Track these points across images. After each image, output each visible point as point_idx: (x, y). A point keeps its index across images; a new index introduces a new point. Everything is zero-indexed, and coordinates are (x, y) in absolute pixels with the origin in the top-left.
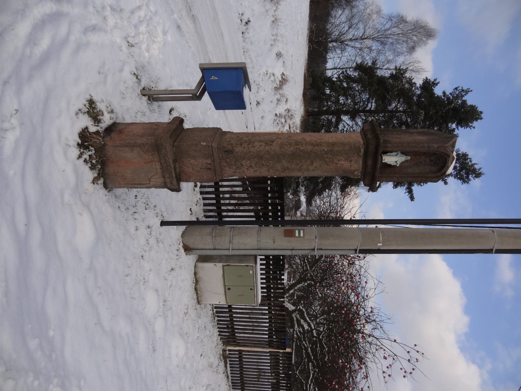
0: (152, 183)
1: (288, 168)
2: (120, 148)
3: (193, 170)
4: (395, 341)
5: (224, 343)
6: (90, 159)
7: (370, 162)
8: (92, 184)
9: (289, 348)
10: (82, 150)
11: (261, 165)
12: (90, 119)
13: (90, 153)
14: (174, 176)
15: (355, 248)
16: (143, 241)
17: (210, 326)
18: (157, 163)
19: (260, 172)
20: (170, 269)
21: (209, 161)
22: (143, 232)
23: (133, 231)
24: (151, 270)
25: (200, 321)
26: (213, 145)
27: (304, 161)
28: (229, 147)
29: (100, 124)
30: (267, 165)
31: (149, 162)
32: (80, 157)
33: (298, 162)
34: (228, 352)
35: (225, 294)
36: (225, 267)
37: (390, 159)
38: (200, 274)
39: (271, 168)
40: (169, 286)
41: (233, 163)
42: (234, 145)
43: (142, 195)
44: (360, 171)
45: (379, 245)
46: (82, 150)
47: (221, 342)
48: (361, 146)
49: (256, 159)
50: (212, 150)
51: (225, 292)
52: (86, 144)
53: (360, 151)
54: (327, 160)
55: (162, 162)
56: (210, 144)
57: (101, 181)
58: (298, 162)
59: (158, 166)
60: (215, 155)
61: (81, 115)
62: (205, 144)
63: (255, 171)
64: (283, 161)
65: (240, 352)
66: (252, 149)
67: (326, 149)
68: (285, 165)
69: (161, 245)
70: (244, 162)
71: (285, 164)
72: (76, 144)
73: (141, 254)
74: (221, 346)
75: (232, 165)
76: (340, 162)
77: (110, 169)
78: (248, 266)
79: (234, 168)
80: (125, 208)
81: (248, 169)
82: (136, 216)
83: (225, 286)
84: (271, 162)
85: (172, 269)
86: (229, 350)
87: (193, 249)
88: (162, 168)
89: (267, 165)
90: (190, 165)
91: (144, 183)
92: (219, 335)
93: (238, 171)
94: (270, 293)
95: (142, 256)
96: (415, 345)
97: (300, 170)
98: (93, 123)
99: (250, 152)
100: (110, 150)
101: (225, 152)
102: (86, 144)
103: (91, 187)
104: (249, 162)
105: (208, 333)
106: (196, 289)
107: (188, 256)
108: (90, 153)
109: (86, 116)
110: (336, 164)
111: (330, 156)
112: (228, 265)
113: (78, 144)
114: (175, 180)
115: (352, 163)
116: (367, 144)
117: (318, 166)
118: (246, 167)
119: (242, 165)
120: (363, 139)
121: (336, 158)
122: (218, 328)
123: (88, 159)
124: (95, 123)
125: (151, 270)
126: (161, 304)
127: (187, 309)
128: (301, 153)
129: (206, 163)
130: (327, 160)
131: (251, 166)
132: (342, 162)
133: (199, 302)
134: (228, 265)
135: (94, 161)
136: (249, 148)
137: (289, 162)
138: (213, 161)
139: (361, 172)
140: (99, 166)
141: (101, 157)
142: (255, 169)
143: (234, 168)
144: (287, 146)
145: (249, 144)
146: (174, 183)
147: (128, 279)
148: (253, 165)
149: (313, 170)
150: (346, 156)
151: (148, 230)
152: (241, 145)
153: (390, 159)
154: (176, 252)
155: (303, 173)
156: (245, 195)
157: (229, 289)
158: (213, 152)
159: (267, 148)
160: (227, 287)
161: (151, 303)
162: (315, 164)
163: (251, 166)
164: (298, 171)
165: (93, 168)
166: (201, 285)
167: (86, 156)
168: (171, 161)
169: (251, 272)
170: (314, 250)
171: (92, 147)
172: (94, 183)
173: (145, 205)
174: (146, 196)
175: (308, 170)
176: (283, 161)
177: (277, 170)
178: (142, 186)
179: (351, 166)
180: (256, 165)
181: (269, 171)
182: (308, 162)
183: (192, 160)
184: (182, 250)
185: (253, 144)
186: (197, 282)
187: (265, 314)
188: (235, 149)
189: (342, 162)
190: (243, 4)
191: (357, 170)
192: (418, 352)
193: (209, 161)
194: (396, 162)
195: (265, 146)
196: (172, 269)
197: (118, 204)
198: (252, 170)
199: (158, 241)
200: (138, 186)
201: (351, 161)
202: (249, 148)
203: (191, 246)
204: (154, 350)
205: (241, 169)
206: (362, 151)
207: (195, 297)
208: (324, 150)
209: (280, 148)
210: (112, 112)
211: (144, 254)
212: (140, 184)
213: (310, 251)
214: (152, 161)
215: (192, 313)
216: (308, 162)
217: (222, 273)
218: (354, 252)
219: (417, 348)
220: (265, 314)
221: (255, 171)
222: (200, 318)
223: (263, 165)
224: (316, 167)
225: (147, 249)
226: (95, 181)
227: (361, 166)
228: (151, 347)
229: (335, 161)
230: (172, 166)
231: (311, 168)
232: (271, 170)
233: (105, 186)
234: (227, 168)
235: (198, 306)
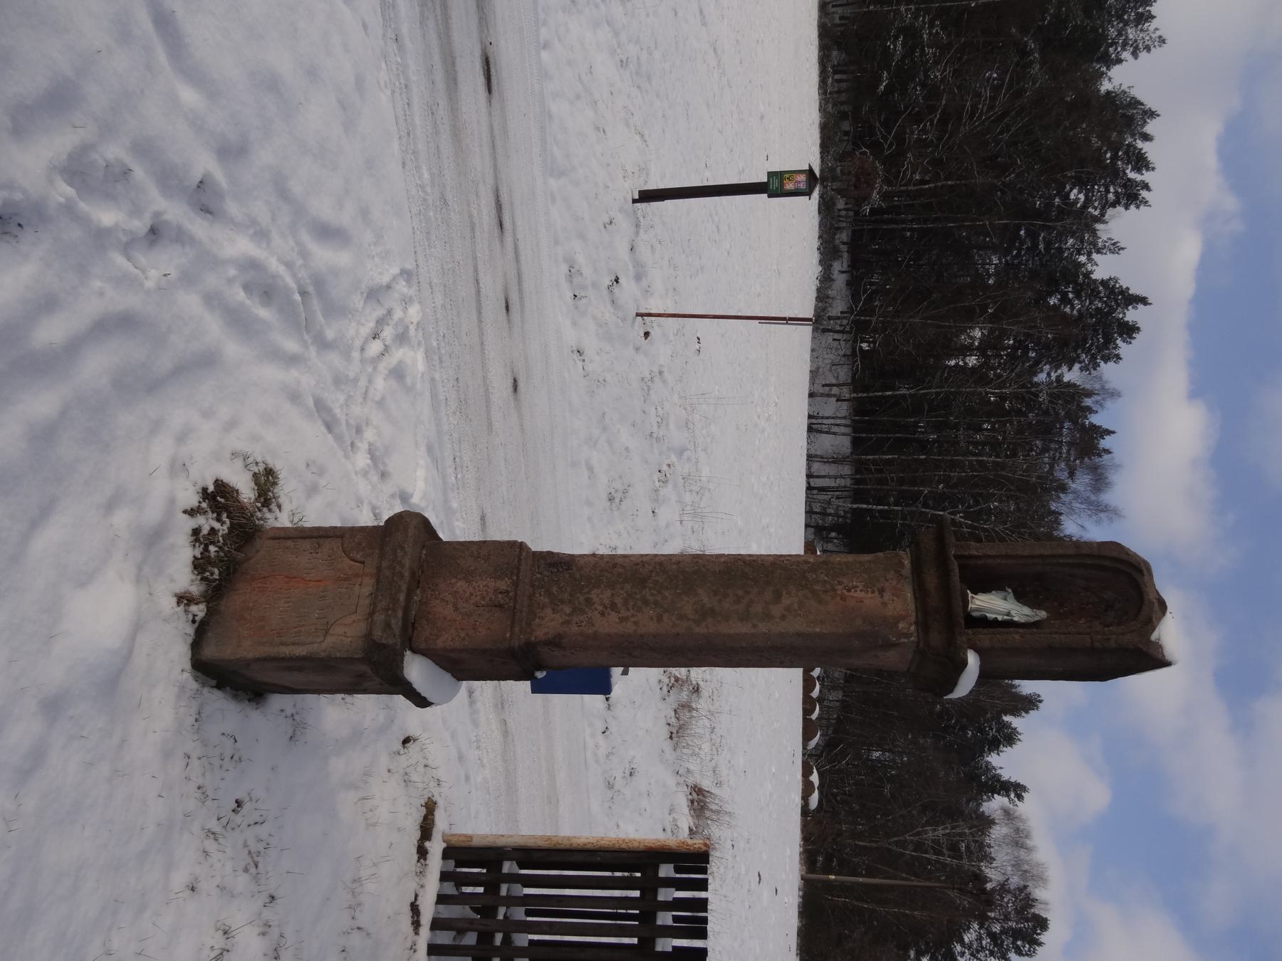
1: (712, 610)
2: (290, 543)
3: (456, 609)
7: (931, 581)
8: (175, 600)
10: (204, 505)
11: (639, 603)
12: (253, 484)
13: (217, 525)
19: (636, 623)
21: (503, 585)
29: (265, 510)
31: (345, 580)
32: (191, 512)
33: (740, 592)
41: (566, 596)
43: (256, 817)
44: (913, 619)
46: (204, 505)
49: (628, 586)
50: (520, 554)
53: (902, 565)
55: (385, 564)
57: (199, 610)
58: (740, 592)
60: (523, 568)
61: (239, 463)
64: (700, 591)
70: (594, 596)
71: (706, 600)
72: (200, 485)
75: (562, 602)
77: (234, 601)
81: (603, 614)
84: (666, 593)
89: (656, 603)
90: (449, 598)
93: (575, 619)
97: (744, 618)
103: (168, 603)
104: (608, 593)
108: (217, 525)
109: (249, 476)
110: (843, 598)
113: (205, 490)
115: (887, 596)
118: (600, 608)
119: (589, 602)
121: (840, 583)
123: (205, 531)
129: (496, 591)
130: (817, 587)
131: (613, 606)
137: (715, 593)
138: (516, 584)
139: (916, 623)
142: (624, 613)
143: (568, 610)
148: (619, 601)
149: (783, 617)
155: (754, 626)
158: (520, 560)
162: (786, 601)
163: (613, 606)
164: (742, 620)
165: (199, 565)
167: (206, 522)
173: (249, 860)
174: (262, 831)
175: (767, 616)
176: (700, 591)
177: (682, 617)
179: (884, 604)
180: (626, 602)
181: (660, 619)
190: (621, 825)
191: (903, 618)
193: (503, 585)
198: (613, 617)
201: (882, 591)
205: (583, 612)
212: (294, 644)
214: (357, 575)
221: (622, 620)
223: (646, 602)
224: (788, 609)
226: (184, 599)
227: (912, 606)
231: (776, 610)
232: (666, 616)
234: (548, 611)
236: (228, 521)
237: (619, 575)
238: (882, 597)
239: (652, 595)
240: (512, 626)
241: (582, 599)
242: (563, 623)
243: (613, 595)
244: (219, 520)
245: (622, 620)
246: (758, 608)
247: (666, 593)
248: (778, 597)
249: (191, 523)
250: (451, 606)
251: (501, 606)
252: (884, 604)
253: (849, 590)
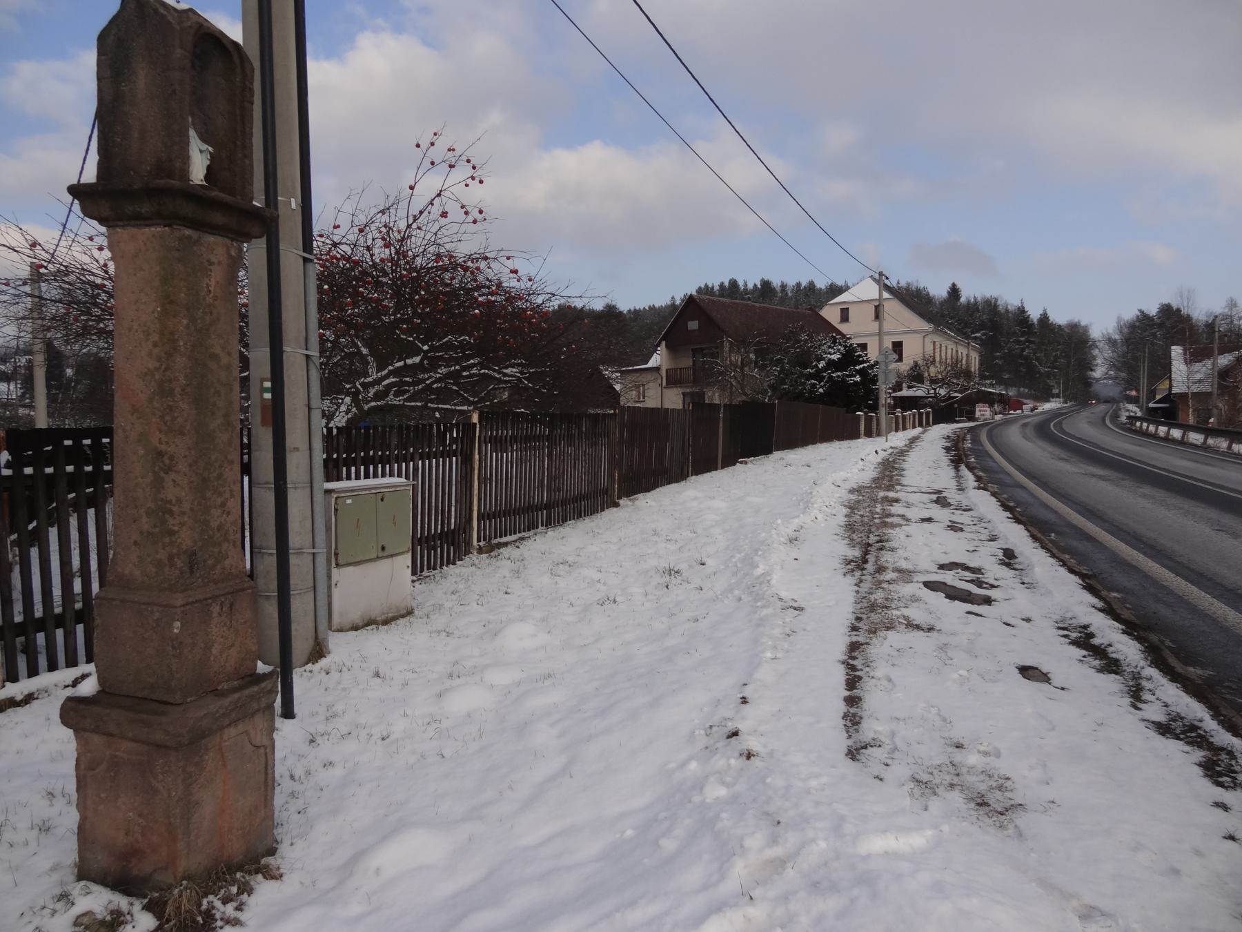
0: (266, 742)
3: (233, 645)
4: (412, 188)
5: (468, 552)
6: (231, 900)
7: (218, 218)
9: (470, 417)
13: (218, 904)
14: (256, 688)
15: (301, 261)
16: (350, 746)
17: (447, 585)
18: (225, 737)
20: (378, 680)
22: (326, 749)
23: (337, 772)
24: (406, 715)
25: (448, 605)
26: (179, 602)
28: (179, 563)
30: (221, 466)
31: (222, 756)
32: (236, 922)
33: (212, 390)
34: (482, 543)
35: (392, 556)
36: (341, 562)
37: (198, 166)
38: (356, 616)
40: (415, 675)
41: (216, 550)
42: (175, 551)
45: (294, 206)
46: (219, 923)
47: (467, 559)
48: (178, 234)
49: (209, 494)
50: (192, 603)
51: (387, 557)
52: (199, 919)
53: (189, 237)
54: (208, 318)
55: (227, 722)
56: (179, 611)
57: (270, 860)
58: (212, 390)
59: (232, 732)
62: (178, 624)
65: (481, 517)
66: (186, 506)
67: (185, 322)
68: (220, 421)
69: (339, 707)
70: (215, 524)
73: (379, 742)
74: (474, 557)
75: (220, 552)
76: (212, 289)
77: (236, 848)
78: (336, 510)
79: (225, 546)
80: (294, 800)
81: (229, 513)
82: (299, 772)
83: (378, 558)
84: (213, 458)
85: (377, 675)
86: (479, 540)
87: (316, 637)
88: (234, 723)
89: (221, 466)
91: (263, 759)
92: (454, 564)
93: (232, 537)
94: (377, 459)
95: (383, 739)
96: (418, 146)
98: (129, 927)
99: (192, 510)
100: (193, 860)
101: (192, 572)
102: (199, 919)
104: (213, 511)
105: (461, 586)
106: (386, 622)
107: (331, 646)
108: (218, 904)
110: (215, 298)
112: (336, 554)
114: (263, 685)
115: (214, 259)
116: (171, 220)
119: (220, 528)
120: (152, 225)
122: (442, 565)
124: (123, 923)
125: (406, 715)
126: (458, 681)
127: (439, 632)
129: (220, 615)
132: (213, 283)
133: (410, 613)
134: (336, 554)
135: (234, 890)
136: (183, 513)
137: (213, 413)
138: (214, 598)
139: (232, 240)
140: (239, 875)
141: (218, 878)
142: (227, 495)
144: (175, 418)
145: (171, 513)
146: (269, 687)
147: (447, 753)
148: (219, 501)
149: (229, 354)
151: (319, 740)
152: (171, 533)
153: (198, 166)
154: (335, 675)
156: (53, 533)
157: (383, 548)
159: (182, 466)
160: (381, 554)
161: (467, 699)
162: (217, 350)
163: (223, 505)
164: (231, 390)
165: (246, 889)
166: (375, 613)
168: (226, 701)
169: (349, 501)
170: (308, 357)
171: (200, 905)
172: (281, 876)
178: (270, 762)
179: (220, 263)
180: (220, 494)
183: (214, 651)
184: (323, 662)
185: (170, 502)
186: (370, 623)
187: (416, 469)
188: (184, 547)
189: (213, 283)
191: (228, 251)
192: (432, 144)
193: (215, 609)
194: (201, 151)
195: (178, 472)
196: (377, 675)
197: (295, 817)
199: (335, 716)
200: (270, 771)
201: (211, 263)
202: (183, 513)
203: (311, 642)
204: (549, 676)
206: (188, 232)
207: (401, 621)
208: (187, 327)
209: (182, 434)
210: (64, 897)
211: (377, 736)
213: (311, 365)
214: (221, 749)
215: (439, 621)
217: (351, 569)
218: (310, 266)
219: (424, 145)
220: (416, 469)
222: (441, 606)
223: (220, 476)
224: (223, 348)
225: (363, 734)
226: (272, 875)
227: (220, 239)
228: (547, 683)
229: (209, 300)
230: (237, 695)
231: (225, 360)
232: (230, 457)
233: (272, 852)
234: (227, 562)
235: (416, 612)
236: (205, 902)
240: (243, 590)
244: (213, 908)
248: (215, 357)
249: (243, 916)
251: (231, 605)
252: (220, 263)
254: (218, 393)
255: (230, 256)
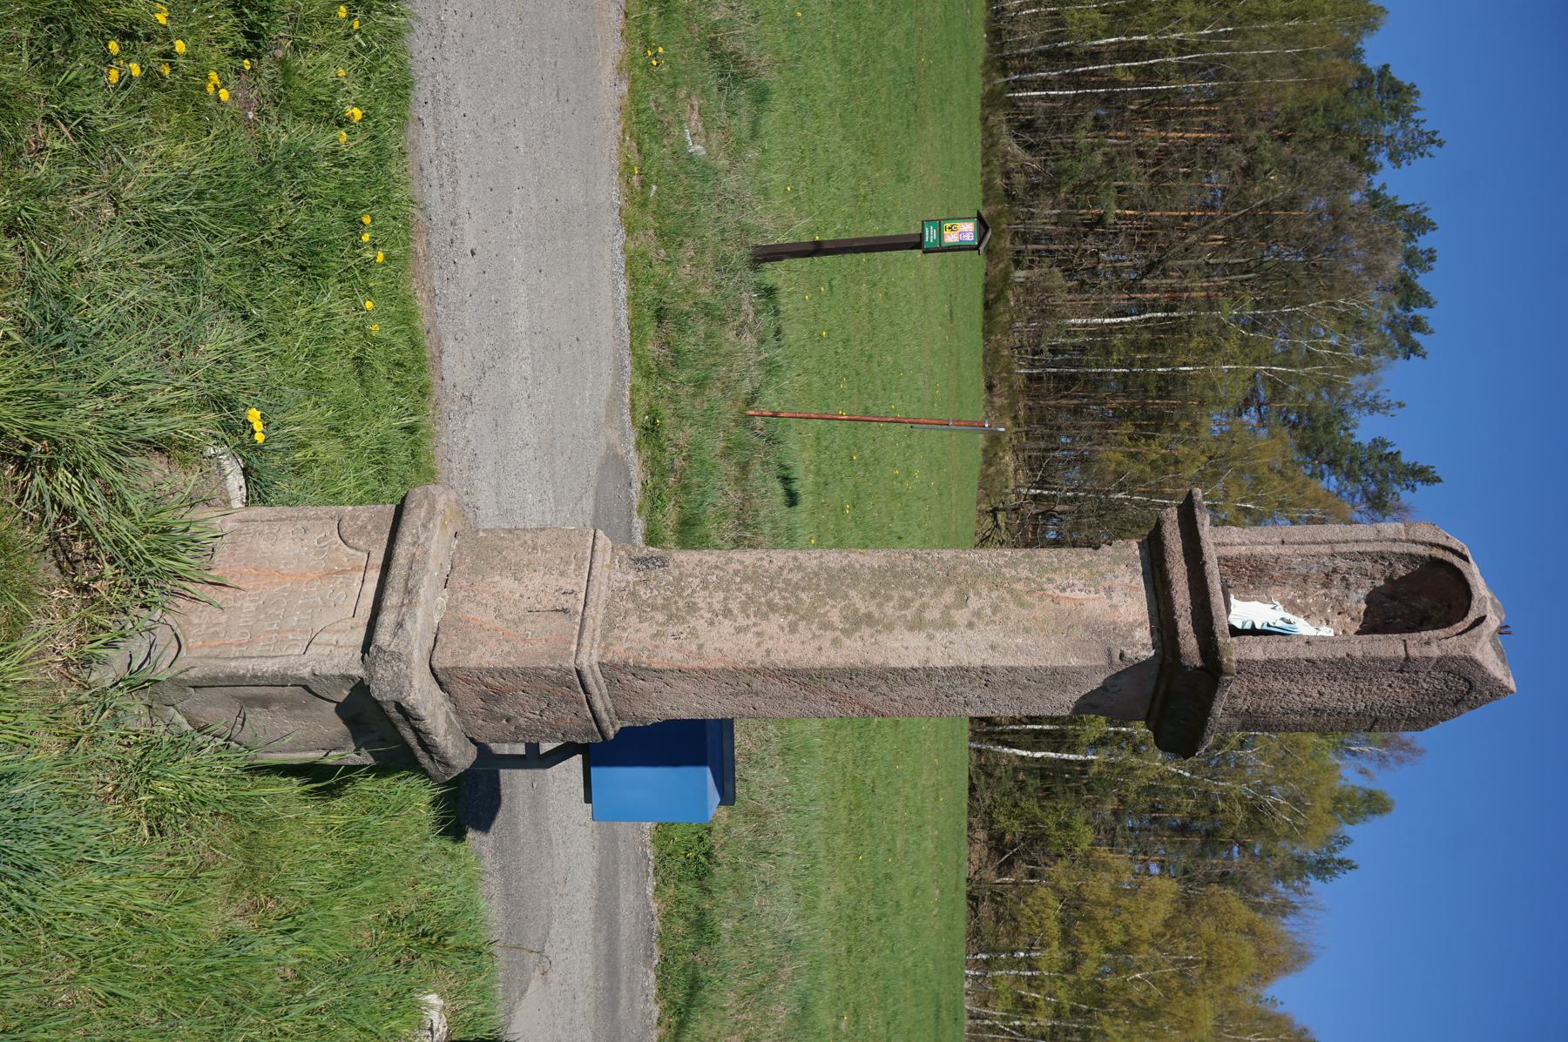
1: (869, 616)
19: (758, 634)
27: (929, 591)
33: (909, 594)
39: (803, 618)
49: (748, 587)
54: (1019, 586)
58: (909, 594)
63: (739, 630)
64: (853, 593)
71: (859, 604)
76: (1068, 593)
81: (712, 623)
84: (803, 595)
89: (788, 608)
90: (492, 602)
93: (671, 629)
97: (916, 625)
111: (1025, 573)
117: (988, 611)
121: (1050, 580)
128: (918, 565)
130: (1019, 586)
137: (873, 595)
148: (734, 606)
149: (971, 625)
150: (1084, 571)
162: (974, 603)
163: (727, 613)
164: (911, 629)
176: (853, 593)
180: (744, 610)
182: (948, 596)
198: (727, 626)
201: (1109, 591)
216: (948, 596)
224: (978, 614)
231: (961, 616)
232: (802, 625)
234: (633, 619)
237: (736, 573)
238: (1110, 598)
239: (784, 598)
241: (681, 604)
242: (654, 636)
243: (725, 599)
245: (739, 630)
246: (933, 614)
247: (803, 595)
248: (962, 600)
250: (491, 612)
252: (1114, 607)
253: (1064, 590)
254: (906, 604)
255: (1132, 627)
